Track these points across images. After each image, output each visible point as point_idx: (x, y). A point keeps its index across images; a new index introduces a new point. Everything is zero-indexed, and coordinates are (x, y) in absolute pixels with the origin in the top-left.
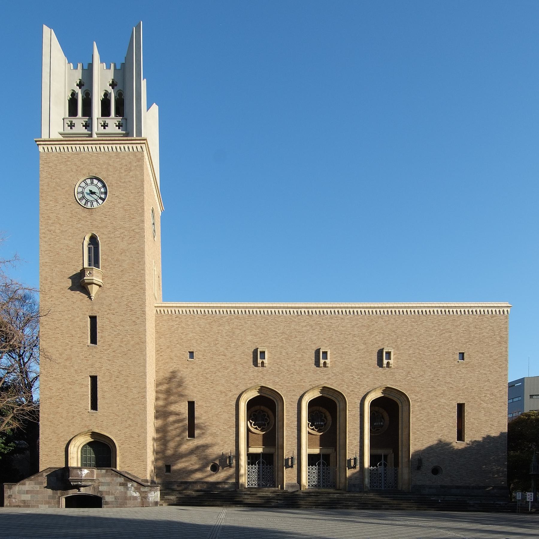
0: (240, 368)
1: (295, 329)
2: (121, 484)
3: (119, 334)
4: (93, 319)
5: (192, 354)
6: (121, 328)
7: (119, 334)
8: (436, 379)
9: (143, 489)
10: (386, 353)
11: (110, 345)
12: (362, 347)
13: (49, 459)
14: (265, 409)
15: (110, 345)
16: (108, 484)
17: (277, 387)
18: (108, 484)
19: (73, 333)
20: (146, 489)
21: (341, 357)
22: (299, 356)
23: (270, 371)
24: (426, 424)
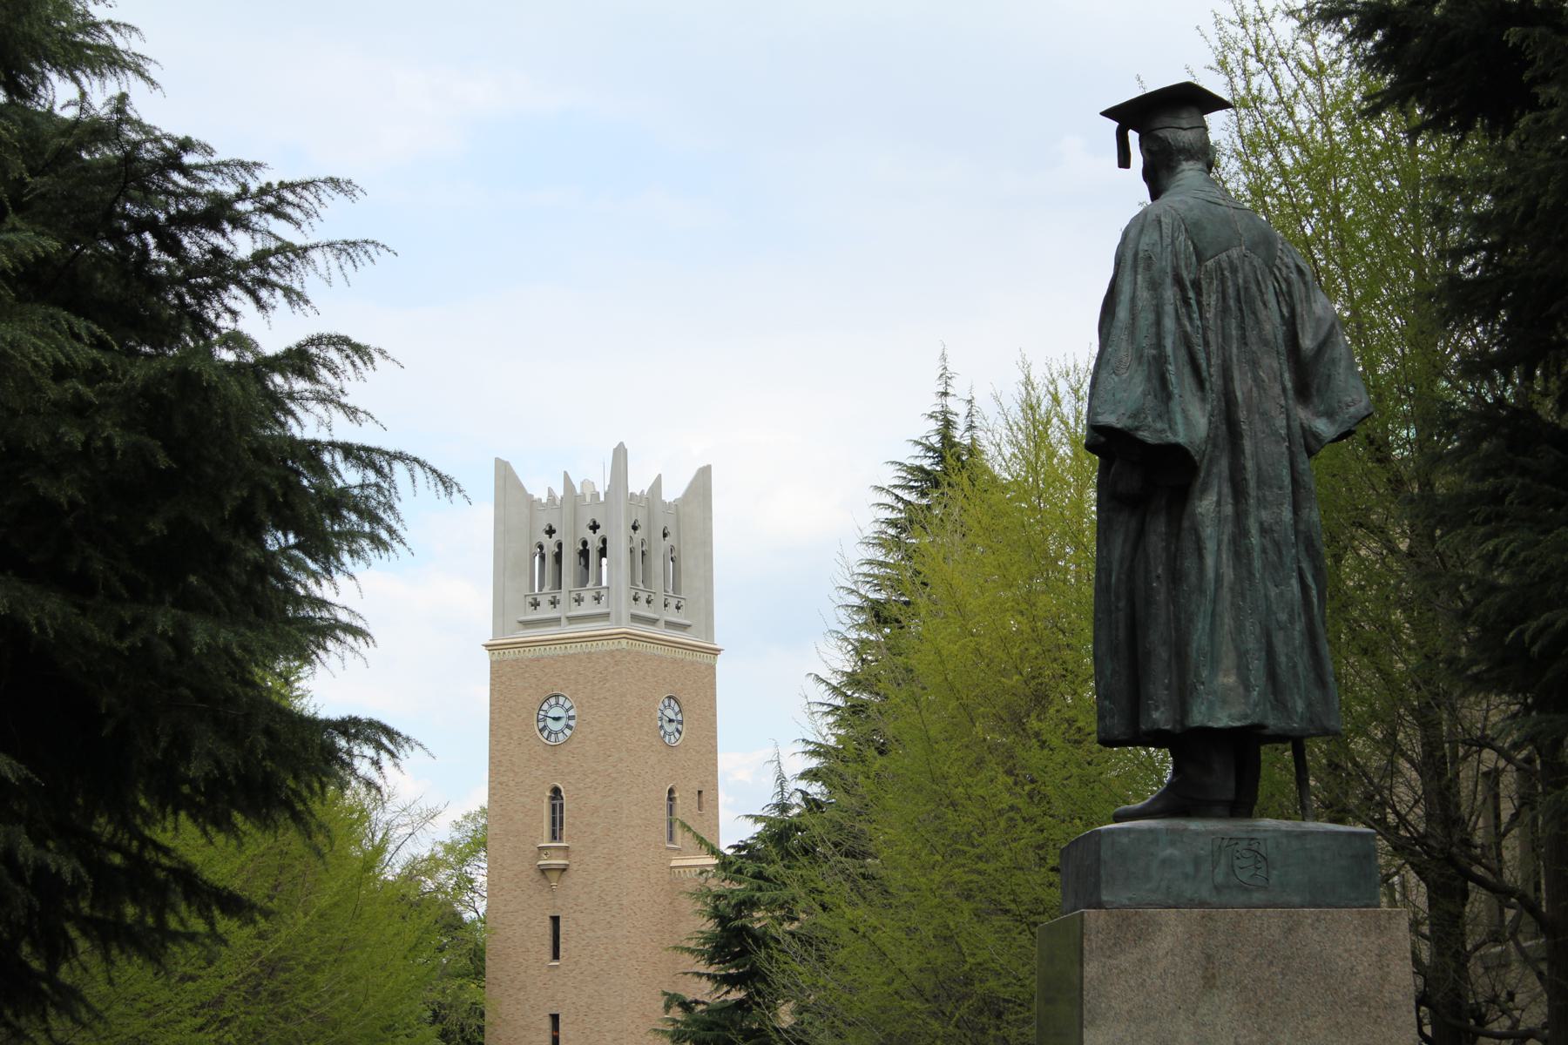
3: (588, 945)
4: (555, 920)
7: (588, 945)
11: (576, 963)
15: (576, 963)
19: (529, 945)
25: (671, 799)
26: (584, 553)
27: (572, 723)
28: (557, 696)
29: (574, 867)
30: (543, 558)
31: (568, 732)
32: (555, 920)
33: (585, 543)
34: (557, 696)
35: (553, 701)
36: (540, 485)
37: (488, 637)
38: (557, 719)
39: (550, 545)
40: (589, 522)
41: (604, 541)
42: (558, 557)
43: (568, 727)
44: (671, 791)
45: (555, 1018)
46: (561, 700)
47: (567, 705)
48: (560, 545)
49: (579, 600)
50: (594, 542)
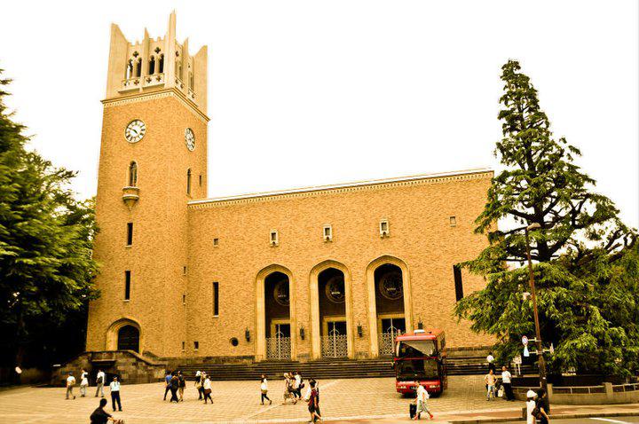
0: (255, 249)
1: (301, 211)
2: (134, 364)
4: (130, 225)
5: (216, 240)
6: (149, 230)
8: (431, 244)
9: (149, 368)
11: (141, 245)
12: (362, 220)
13: (91, 345)
14: (277, 284)
15: (141, 245)
16: (124, 364)
18: (124, 364)
24: (425, 288)
25: (189, 175)
26: (152, 64)
27: (143, 132)
28: (136, 121)
29: (141, 199)
30: (131, 71)
31: (141, 137)
33: (153, 58)
34: (136, 121)
35: (134, 123)
36: (134, 36)
39: (135, 61)
40: (155, 48)
41: (162, 56)
42: (139, 66)
44: (189, 171)
45: (128, 274)
46: (138, 122)
47: (142, 124)
48: (140, 60)
49: (149, 81)
50: (157, 57)
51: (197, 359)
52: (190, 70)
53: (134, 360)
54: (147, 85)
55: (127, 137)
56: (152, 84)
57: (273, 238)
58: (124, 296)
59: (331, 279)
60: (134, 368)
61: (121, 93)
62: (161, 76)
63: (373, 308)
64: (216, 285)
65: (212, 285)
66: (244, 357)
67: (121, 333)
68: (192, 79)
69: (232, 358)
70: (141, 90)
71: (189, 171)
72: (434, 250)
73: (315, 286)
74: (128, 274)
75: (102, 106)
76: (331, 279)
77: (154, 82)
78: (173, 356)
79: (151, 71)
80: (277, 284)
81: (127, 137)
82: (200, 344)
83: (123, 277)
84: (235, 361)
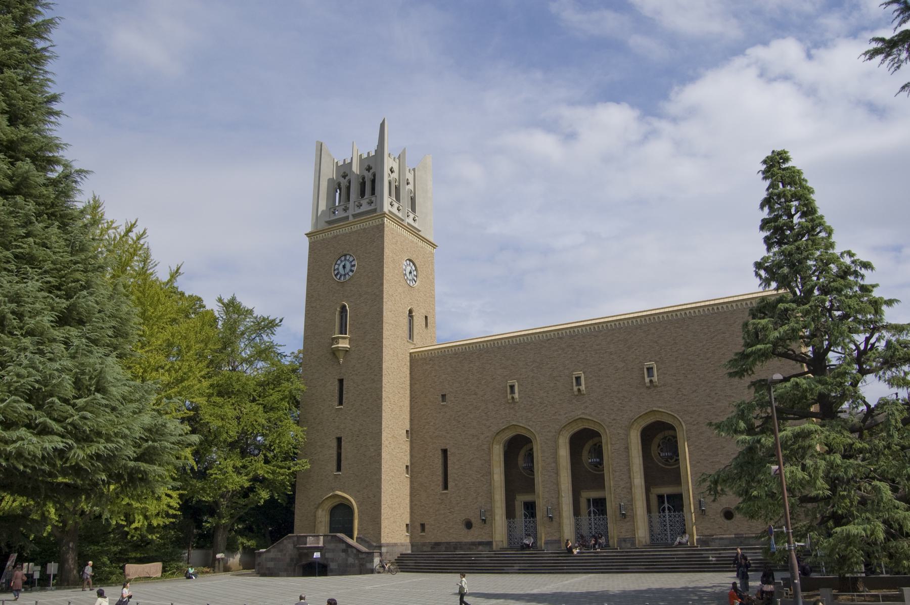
2: (344, 551)
4: (341, 381)
9: (361, 556)
10: (648, 369)
14: (518, 449)
17: (531, 423)
20: (364, 556)
21: (599, 380)
22: (552, 385)
23: (522, 406)
26: (363, 184)
31: (351, 274)
32: (341, 381)
33: (364, 178)
34: (345, 255)
35: (343, 258)
37: (309, 229)
38: (344, 267)
39: (344, 182)
41: (374, 175)
43: (352, 271)
44: (410, 312)
45: (339, 440)
47: (351, 259)
48: (350, 183)
49: (360, 206)
50: (368, 176)
51: (424, 544)
52: (411, 187)
53: (343, 546)
54: (358, 211)
55: (336, 275)
56: (363, 209)
57: (512, 391)
58: (335, 468)
59: (586, 442)
60: (343, 555)
61: (329, 223)
62: (373, 199)
63: (639, 480)
64: (445, 452)
65: (440, 452)
66: (480, 543)
67: (333, 511)
68: (413, 200)
69: (466, 544)
70: (351, 218)
71: (410, 312)
72: (718, 401)
73: (564, 453)
74: (339, 440)
75: (307, 240)
76: (586, 442)
77: (365, 207)
78: (394, 541)
79: (362, 194)
80: (518, 449)
81: (336, 275)
82: (427, 527)
83: (334, 444)
84: (470, 549)
